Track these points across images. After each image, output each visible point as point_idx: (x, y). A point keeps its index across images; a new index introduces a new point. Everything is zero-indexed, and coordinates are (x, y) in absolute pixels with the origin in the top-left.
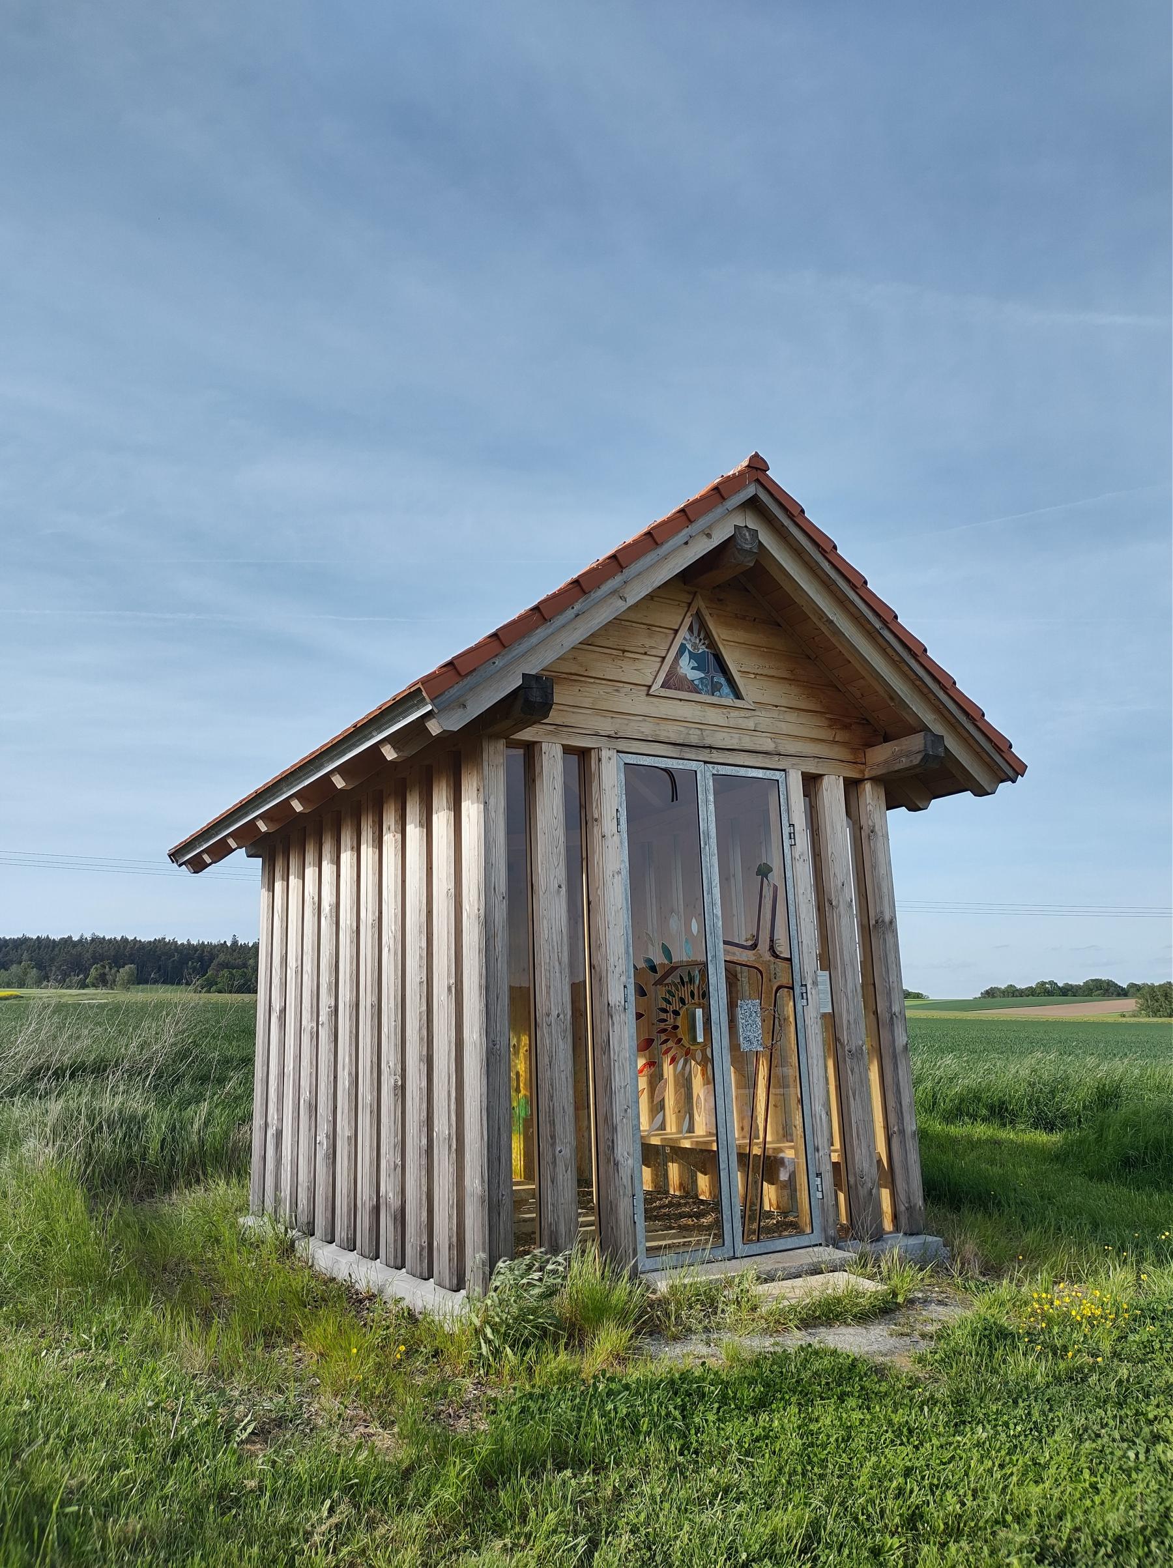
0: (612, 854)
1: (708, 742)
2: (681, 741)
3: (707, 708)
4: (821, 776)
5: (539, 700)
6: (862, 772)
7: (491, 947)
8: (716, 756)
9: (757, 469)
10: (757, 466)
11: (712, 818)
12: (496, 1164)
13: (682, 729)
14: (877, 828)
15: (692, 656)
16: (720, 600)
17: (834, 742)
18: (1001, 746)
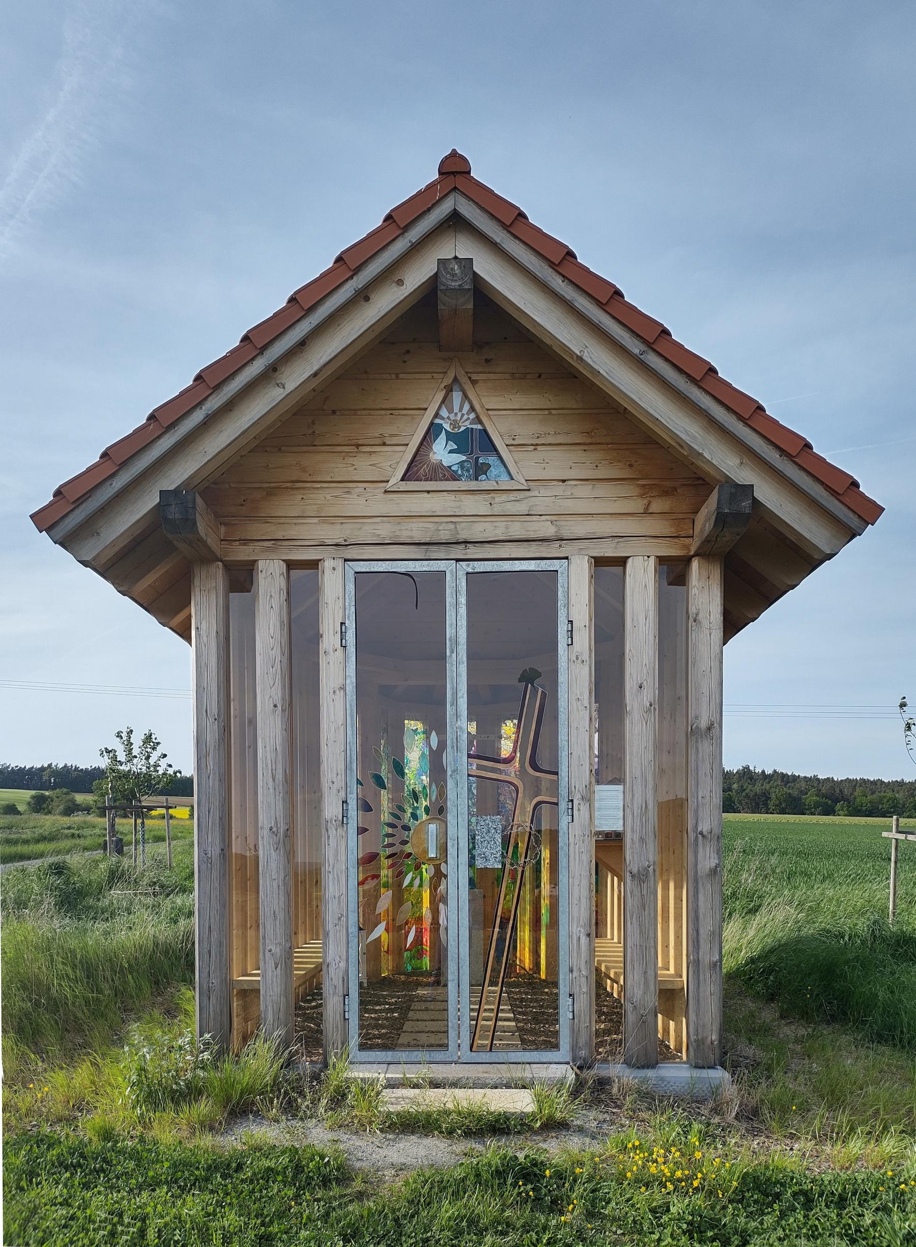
0: (337, 670)
1: (463, 536)
2: (427, 540)
3: (463, 497)
4: (256, 561)
5: (178, 516)
6: (687, 547)
7: (203, 766)
8: (473, 552)
9: (454, 173)
10: (454, 170)
11: (463, 622)
12: (206, 956)
13: (429, 525)
14: (700, 617)
15: (450, 437)
16: (487, 361)
17: (646, 512)
18: (846, 487)
